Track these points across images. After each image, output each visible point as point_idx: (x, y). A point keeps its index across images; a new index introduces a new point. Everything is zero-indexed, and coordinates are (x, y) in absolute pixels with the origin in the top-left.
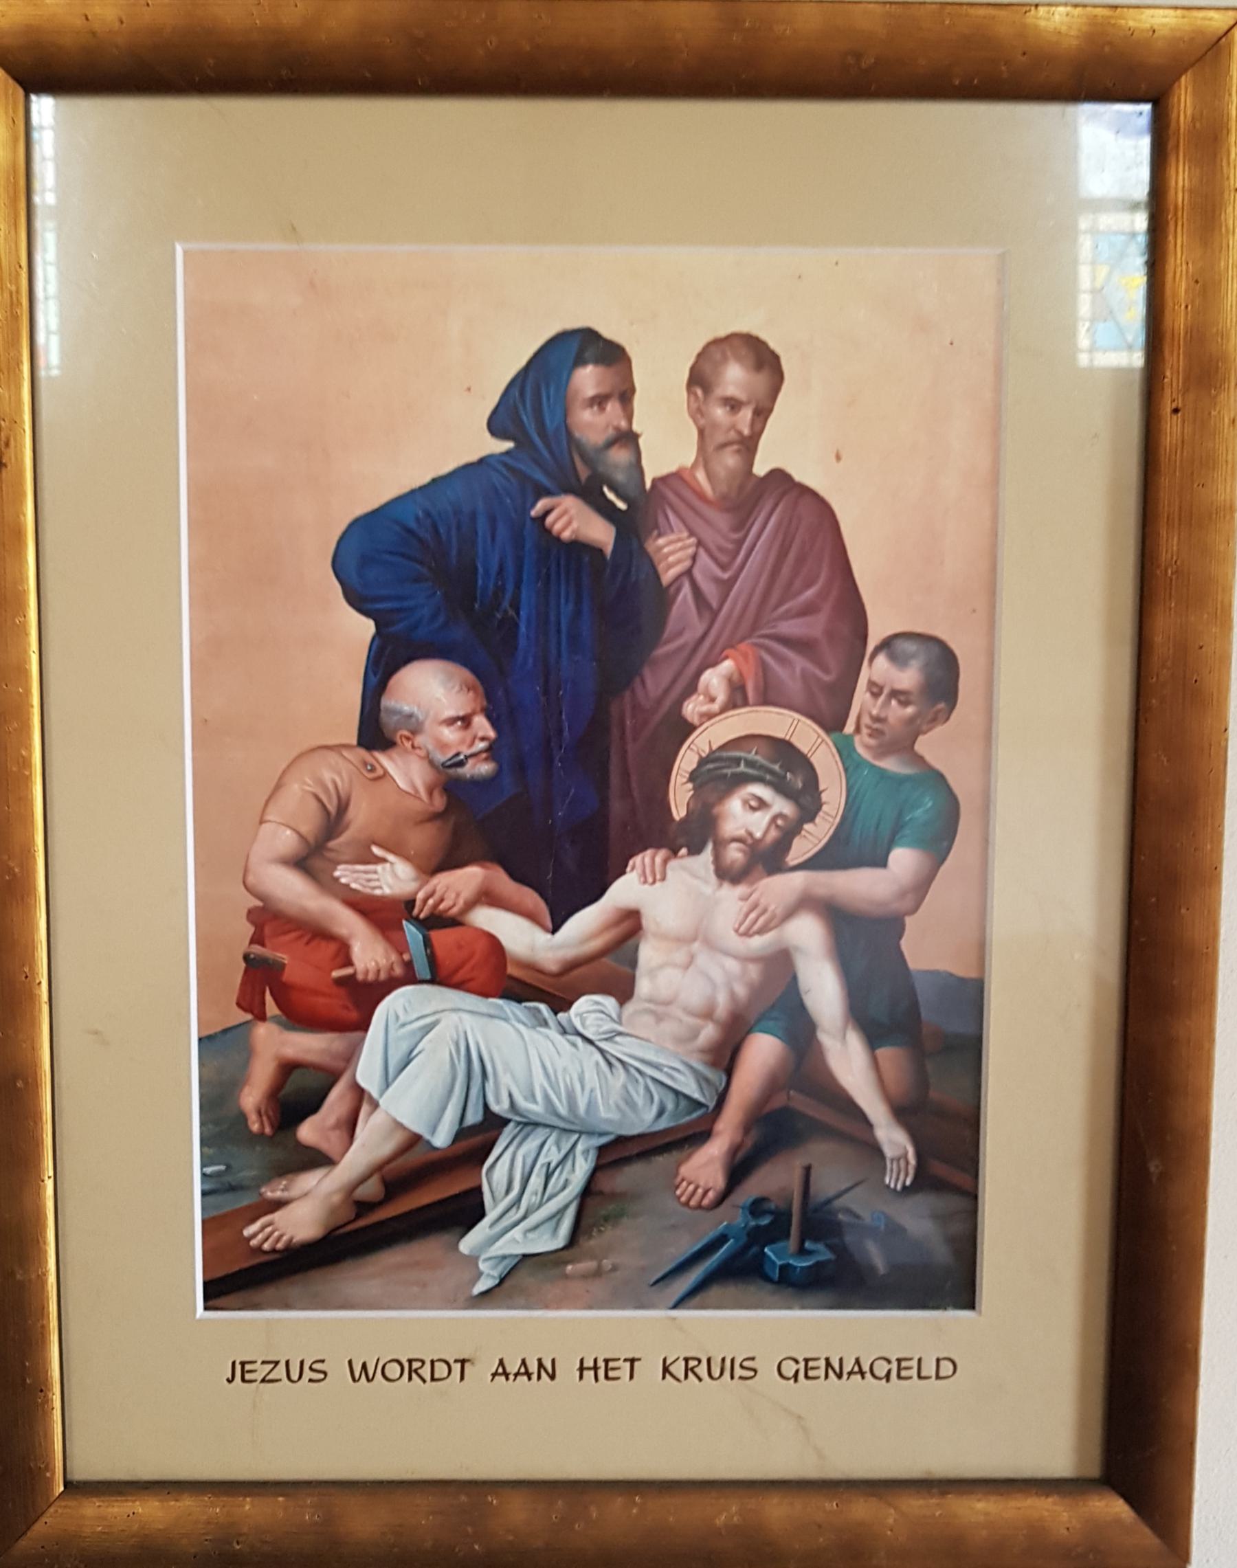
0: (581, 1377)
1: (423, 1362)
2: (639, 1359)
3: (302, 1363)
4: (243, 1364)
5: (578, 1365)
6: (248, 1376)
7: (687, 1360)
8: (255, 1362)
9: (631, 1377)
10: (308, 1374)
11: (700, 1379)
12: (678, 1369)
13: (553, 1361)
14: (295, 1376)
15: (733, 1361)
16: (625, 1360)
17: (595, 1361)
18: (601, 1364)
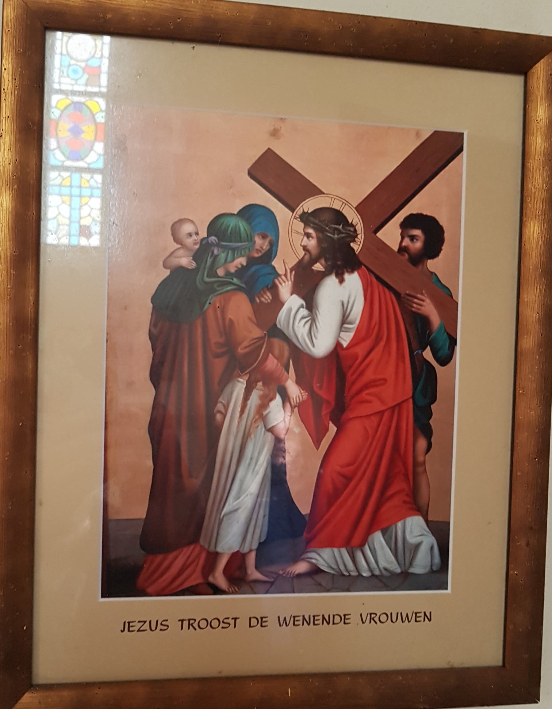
1: (376, 614)
3: (157, 621)
4: (129, 623)
6: (131, 629)
8: (135, 622)
13: (430, 613)
14: (153, 628)
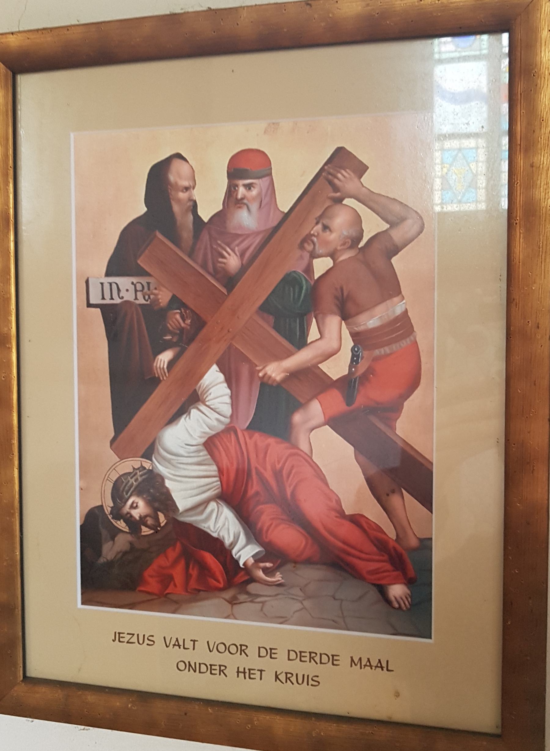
0: (238, 676)
2: (264, 671)
3: (144, 635)
4: (119, 633)
5: (236, 670)
7: (286, 673)
8: (124, 633)
9: (261, 679)
10: (147, 641)
11: (293, 684)
12: (282, 677)
14: (141, 642)
15: (308, 676)
16: (258, 670)
17: (244, 669)
18: (247, 671)
